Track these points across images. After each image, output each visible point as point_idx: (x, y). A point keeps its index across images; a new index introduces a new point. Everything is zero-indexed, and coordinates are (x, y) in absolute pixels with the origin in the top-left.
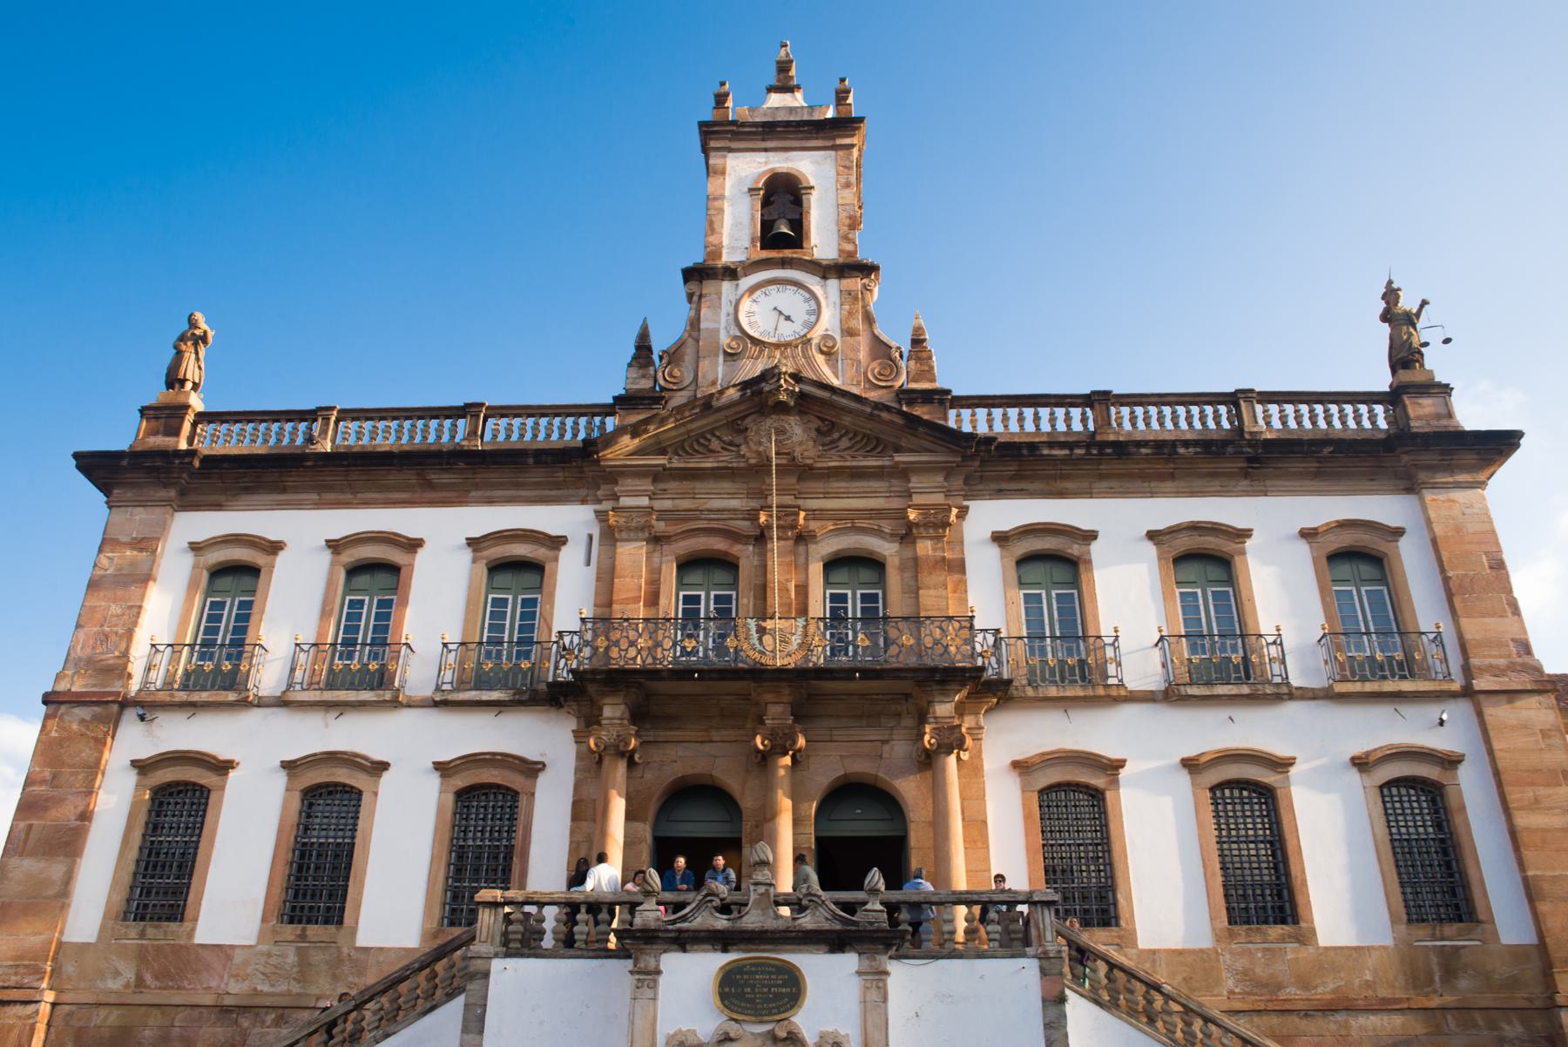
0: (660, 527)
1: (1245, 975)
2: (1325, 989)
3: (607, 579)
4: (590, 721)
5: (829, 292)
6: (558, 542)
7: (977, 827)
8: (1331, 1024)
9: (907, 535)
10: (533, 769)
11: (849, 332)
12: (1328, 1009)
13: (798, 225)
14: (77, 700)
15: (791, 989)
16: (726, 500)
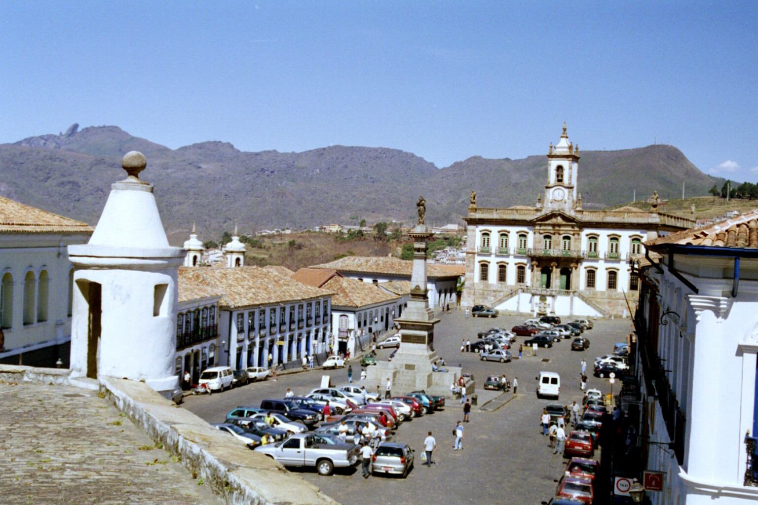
0: (541, 231)
1: (609, 295)
2: (617, 297)
3: (535, 238)
4: (532, 260)
5: (566, 191)
6: (527, 233)
7: (578, 275)
8: (615, 301)
9: (574, 235)
10: (526, 265)
11: (568, 199)
12: (617, 299)
13: (562, 176)
14: (470, 253)
15: (545, 300)
16: (550, 228)
